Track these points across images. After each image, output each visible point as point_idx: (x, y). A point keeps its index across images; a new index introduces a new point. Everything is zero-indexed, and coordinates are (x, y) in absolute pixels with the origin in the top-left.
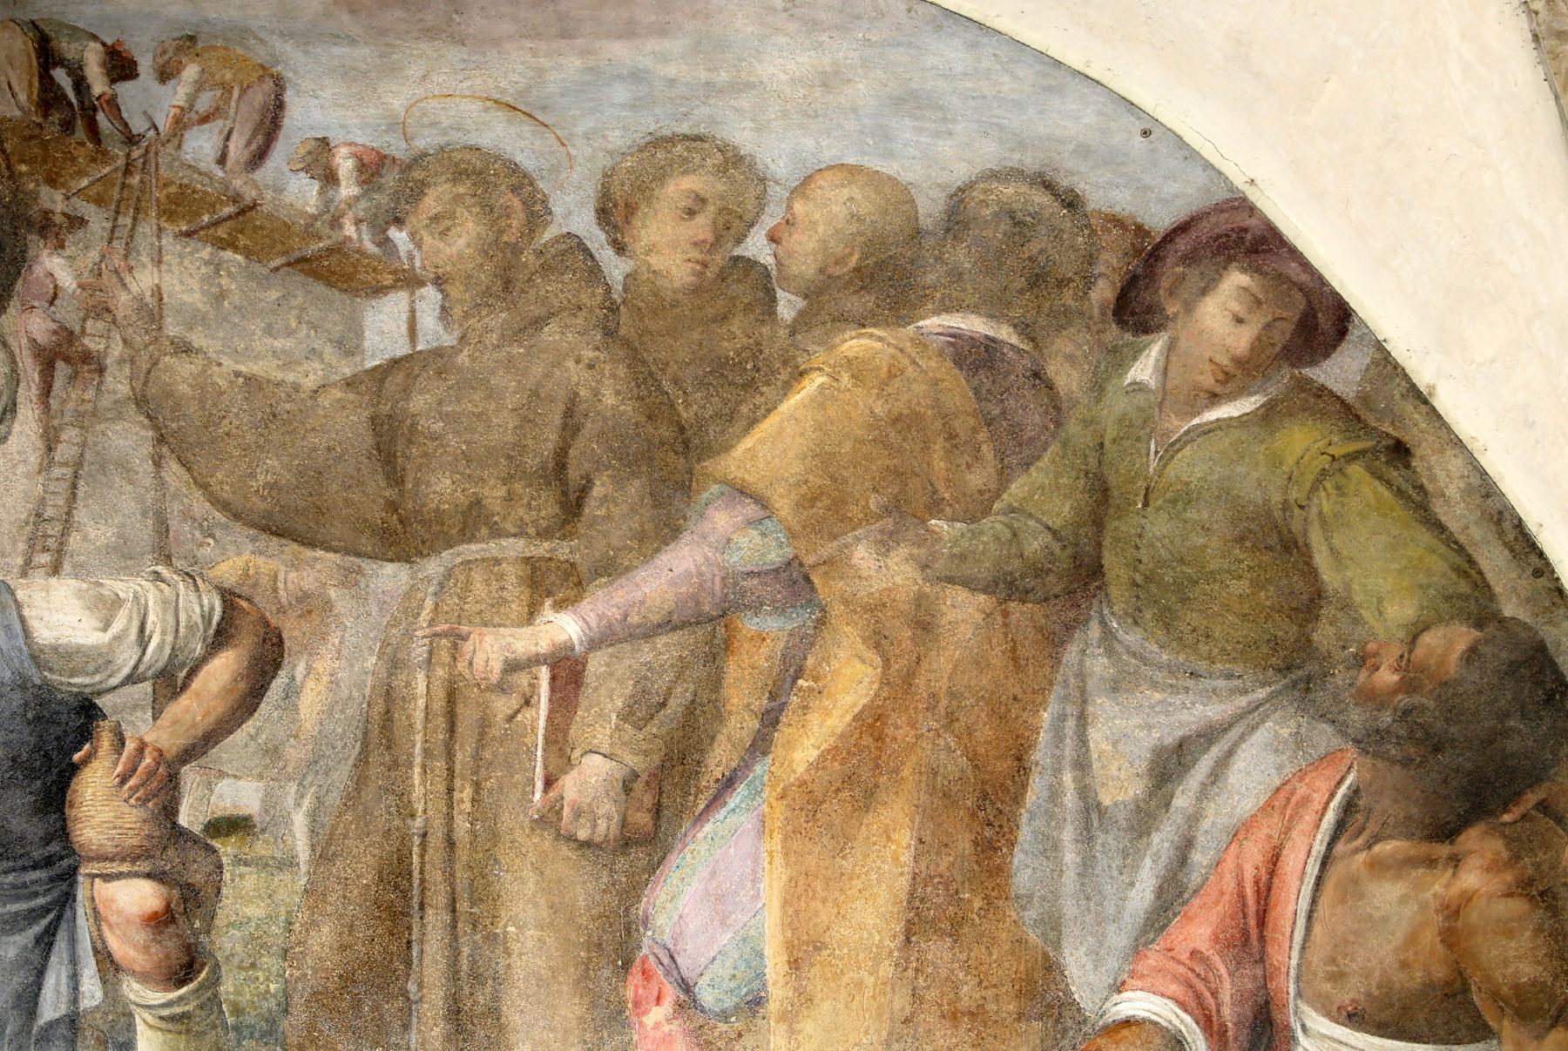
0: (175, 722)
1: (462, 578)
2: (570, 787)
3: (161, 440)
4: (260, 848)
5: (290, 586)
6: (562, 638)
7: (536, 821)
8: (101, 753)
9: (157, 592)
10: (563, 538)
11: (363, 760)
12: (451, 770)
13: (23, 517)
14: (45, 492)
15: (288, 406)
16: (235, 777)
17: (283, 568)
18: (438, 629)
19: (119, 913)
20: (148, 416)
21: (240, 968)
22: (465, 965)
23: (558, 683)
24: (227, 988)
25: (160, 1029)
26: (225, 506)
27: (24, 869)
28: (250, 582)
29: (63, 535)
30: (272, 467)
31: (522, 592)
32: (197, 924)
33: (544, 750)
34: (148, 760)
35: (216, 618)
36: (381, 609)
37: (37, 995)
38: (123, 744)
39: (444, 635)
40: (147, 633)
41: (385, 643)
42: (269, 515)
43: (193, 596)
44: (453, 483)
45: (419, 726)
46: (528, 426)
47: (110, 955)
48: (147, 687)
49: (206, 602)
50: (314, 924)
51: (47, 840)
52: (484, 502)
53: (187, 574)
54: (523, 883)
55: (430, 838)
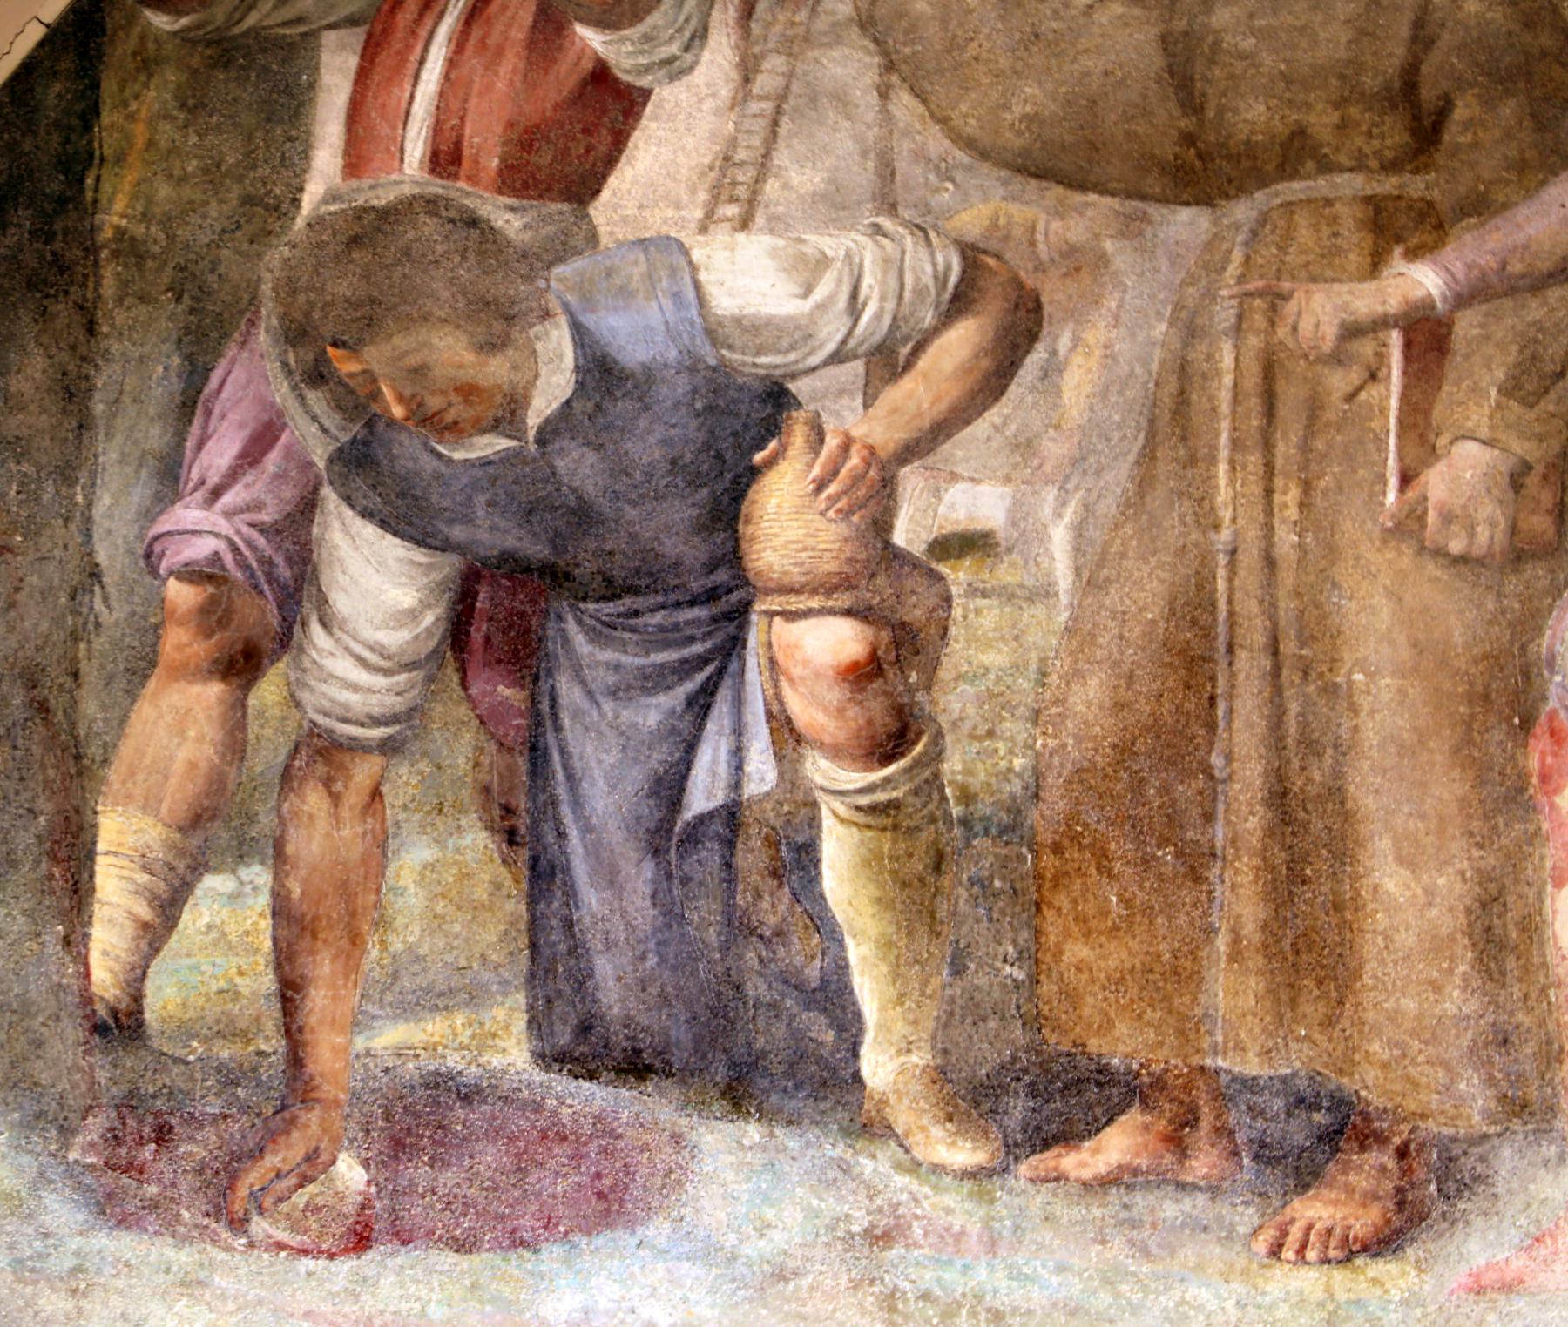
0: (894, 411)
1: (1282, 223)
2: (1437, 483)
3: (890, 67)
4: (1005, 573)
5: (1052, 237)
6: (1419, 293)
7: (1389, 530)
8: (791, 452)
9: (875, 248)
10: (1416, 171)
11: (1148, 455)
12: (1269, 468)
13: (707, 161)
14: (737, 130)
15: (1054, 25)
16: (972, 480)
17: (1043, 217)
18: (1250, 287)
19: (806, 663)
20: (876, 40)
21: (973, 737)
22: (1292, 726)
23: (1415, 351)
24: (952, 766)
25: (856, 824)
26: (969, 144)
27: (678, 605)
28: (999, 234)
29: (757, 181)
30: (1031, 96)
31: (1363, 239)
32: (914, 677)
33: (1399, 437)
34: (855, 460)
35: (953, 279)
36: (1173, 264)
37: (684, 777)
38: (822, 441)
39: (1260, 294)
40: (861, 299)
41: (1178, 306)
42: (1026, 152)
43: (923, 253)
44: (1269, 108)
45: (1225, 408)
46: (1365, 40)
47: (789, 721)
48: (858, 366)
49: (940, 259)
50: (1078, 675)
51: (711, 567)
52: (1310, 131)
53: (917, 226)
54: (1373, 614)
55: (1240, 556)
